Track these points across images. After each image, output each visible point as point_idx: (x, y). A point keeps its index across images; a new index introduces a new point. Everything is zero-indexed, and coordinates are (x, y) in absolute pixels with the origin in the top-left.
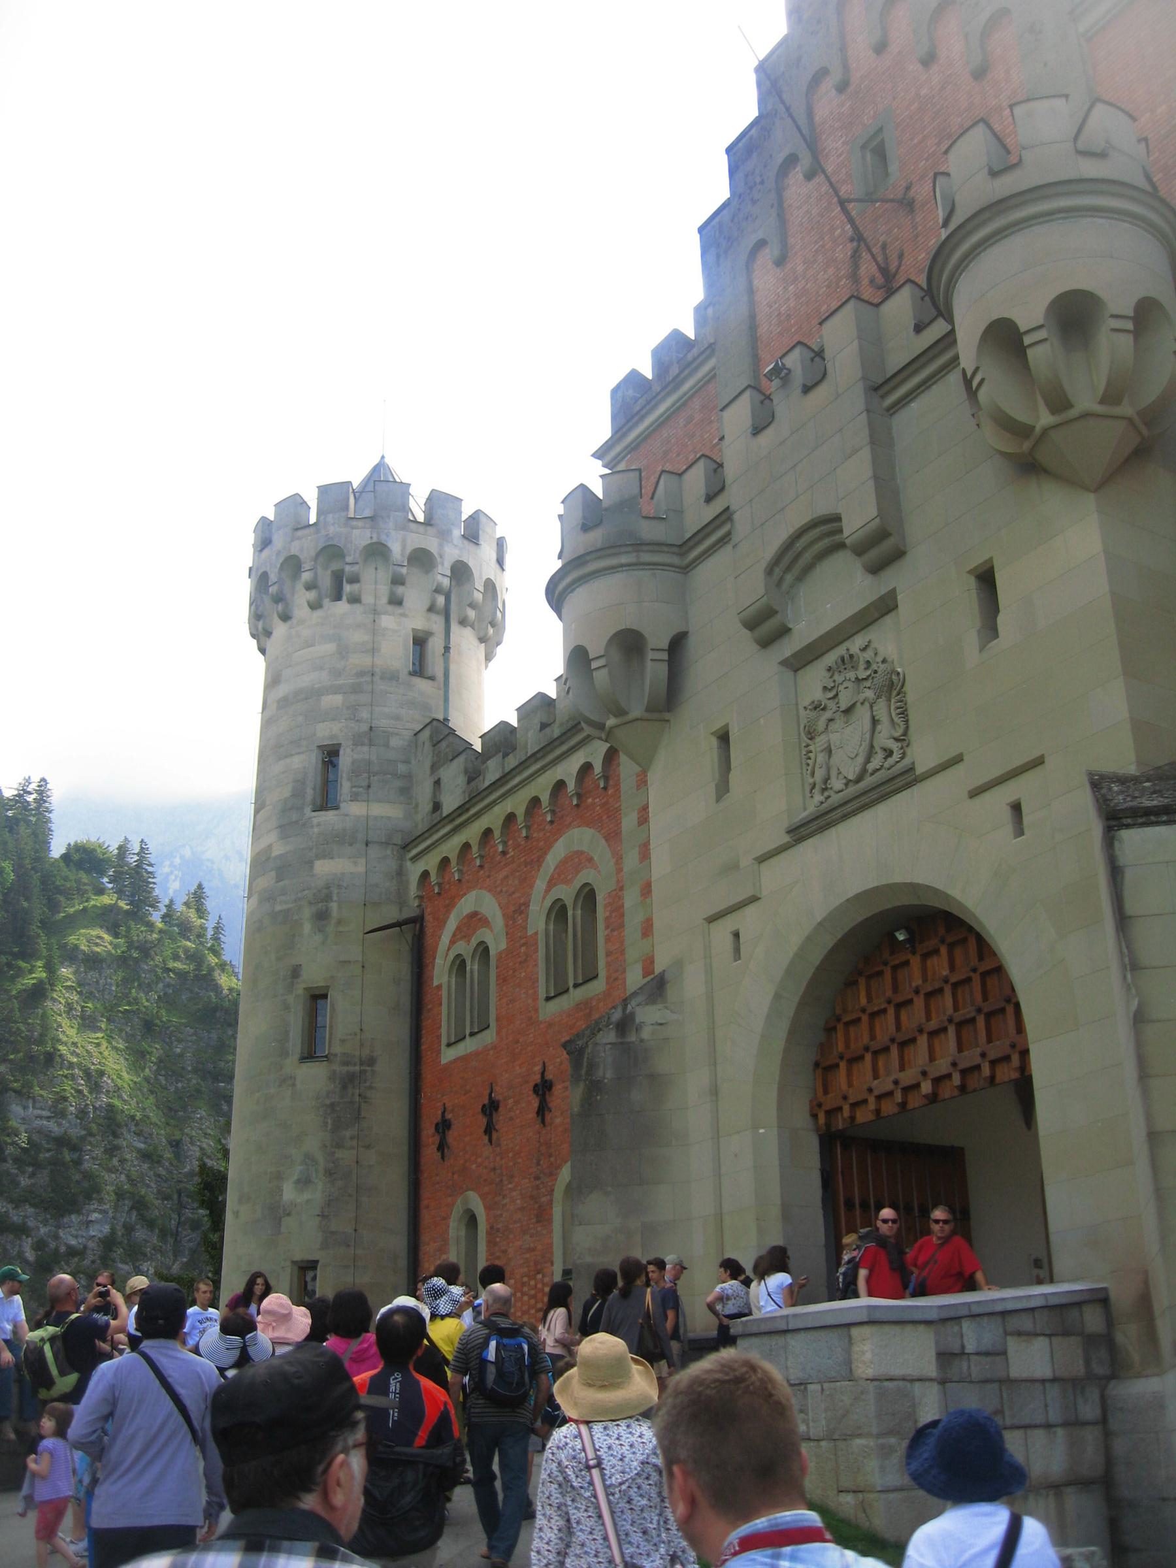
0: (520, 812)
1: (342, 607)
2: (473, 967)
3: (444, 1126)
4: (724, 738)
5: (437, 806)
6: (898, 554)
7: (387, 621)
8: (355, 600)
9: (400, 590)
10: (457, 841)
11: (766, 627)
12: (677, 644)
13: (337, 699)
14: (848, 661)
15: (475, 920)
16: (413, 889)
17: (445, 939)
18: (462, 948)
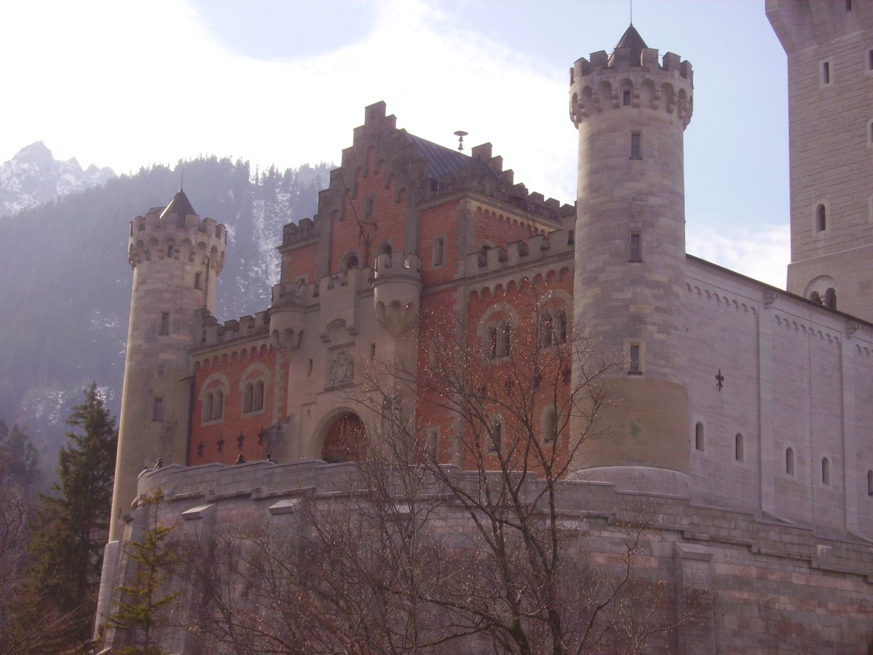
0: (239, 352)
1: (171, 260)
2: (216, 397)
3: (201, 447)
4: (311, 361)
5: (204, 340)
6: (357, 334)
7: (188, 268)
8: (177, 258)
9: (193, 256)
10: (213, 355)
11: (325, 339)
12: (302, 332)
13: (169, 295)
14: (343, 353)
15: (217, 382)
16: (192, 367)
17: (204, 386)
18: (211, 390)
